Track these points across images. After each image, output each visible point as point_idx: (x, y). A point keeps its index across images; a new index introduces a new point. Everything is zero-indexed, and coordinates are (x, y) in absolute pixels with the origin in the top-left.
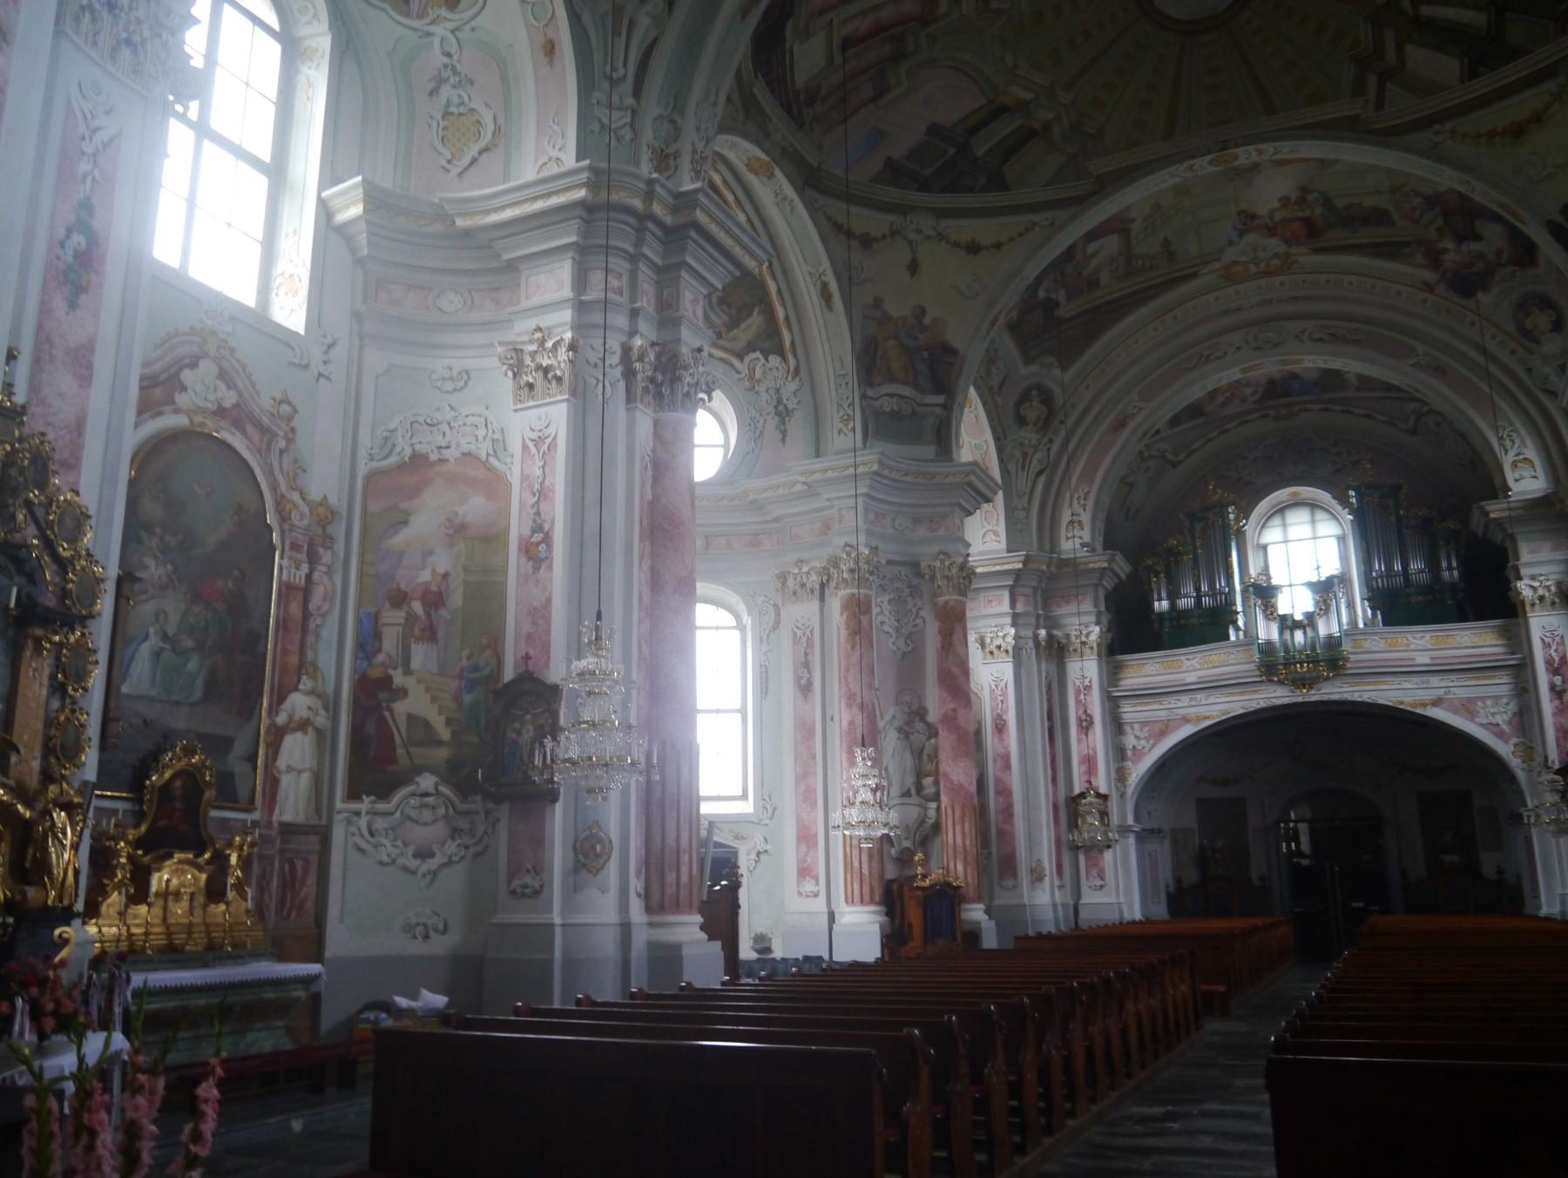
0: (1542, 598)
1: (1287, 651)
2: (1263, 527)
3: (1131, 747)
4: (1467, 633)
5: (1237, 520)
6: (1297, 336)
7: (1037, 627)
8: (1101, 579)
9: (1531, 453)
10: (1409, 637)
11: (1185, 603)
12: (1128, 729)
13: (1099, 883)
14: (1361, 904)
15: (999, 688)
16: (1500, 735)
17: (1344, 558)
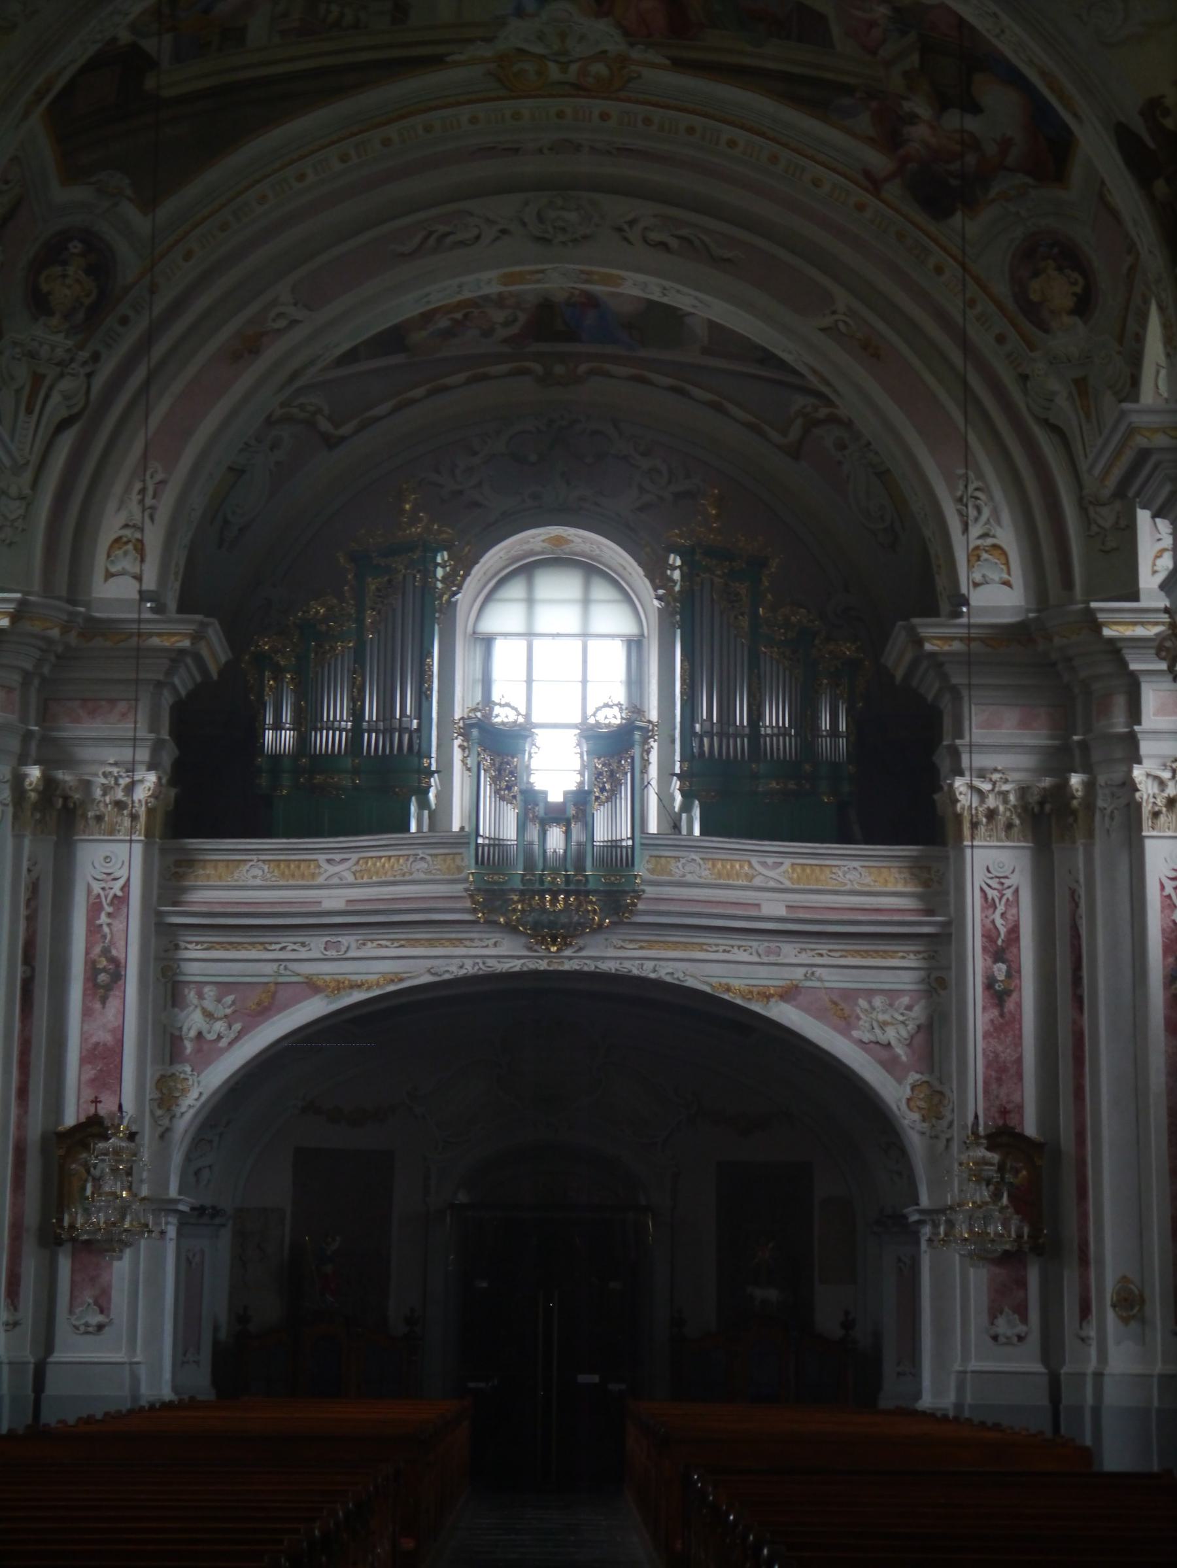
0: (991, 814)
1: (529, 865)
2: (488, 599)
3: (193, 1034)
4: (856, 864)
5: (449, 579)
6: (620, 230)
7: (23, 760)
8: (170, 672)
9: (1007, 536)
10: (754, 861)
11: (327, 741)
12: (191, 996)
13: (96, 1319)
14: (595, 1379)
16: (890, 1065)
17: (635, 682)
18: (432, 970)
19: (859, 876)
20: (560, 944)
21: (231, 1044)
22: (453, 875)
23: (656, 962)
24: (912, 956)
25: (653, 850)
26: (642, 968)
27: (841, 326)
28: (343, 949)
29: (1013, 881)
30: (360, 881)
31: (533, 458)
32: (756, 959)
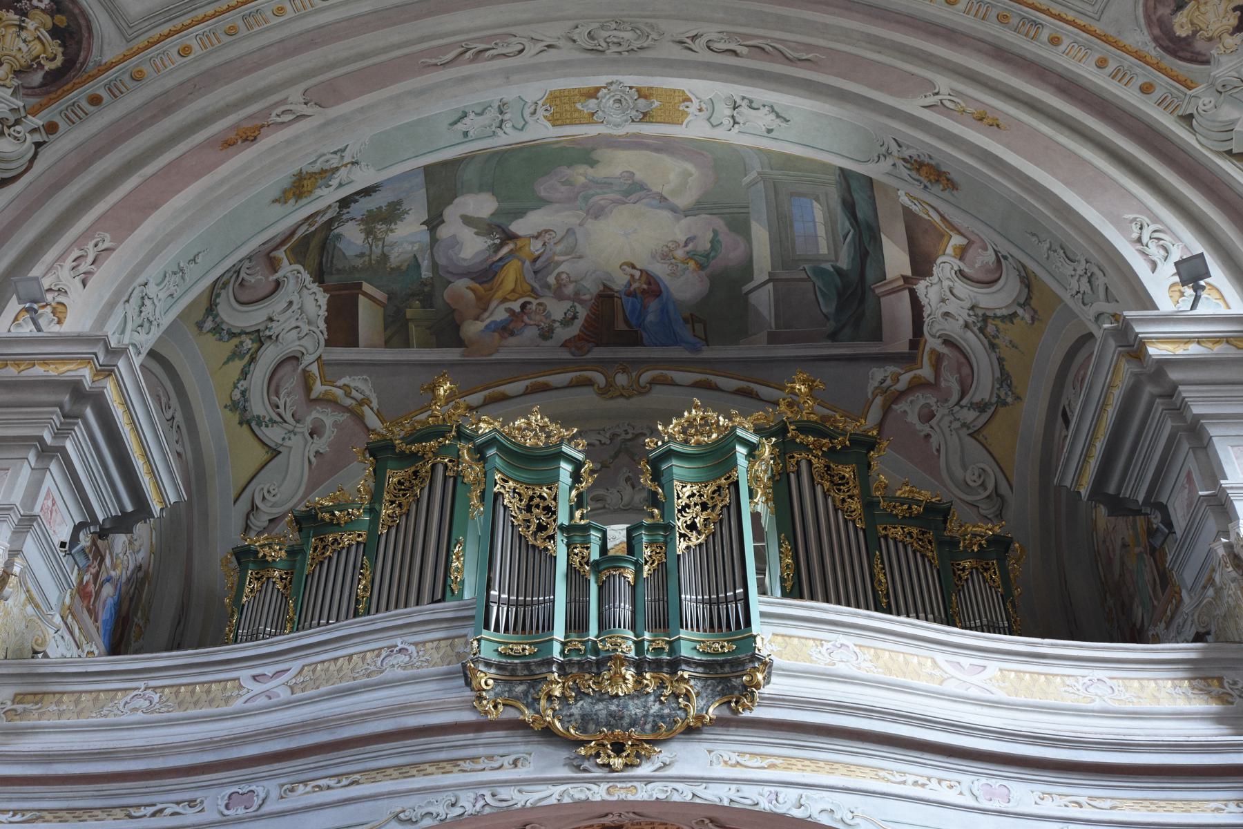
6: (681, 42)
18: (402, 815)
19: (1110, 691)
20: (628, 755)
22: (448, 664)
23: (800, 791)
24: (1232, 807)
25: (779, 625)
26: (776, 800)
27: (947, 103)
28: (257, 802)
30: (299, 695)
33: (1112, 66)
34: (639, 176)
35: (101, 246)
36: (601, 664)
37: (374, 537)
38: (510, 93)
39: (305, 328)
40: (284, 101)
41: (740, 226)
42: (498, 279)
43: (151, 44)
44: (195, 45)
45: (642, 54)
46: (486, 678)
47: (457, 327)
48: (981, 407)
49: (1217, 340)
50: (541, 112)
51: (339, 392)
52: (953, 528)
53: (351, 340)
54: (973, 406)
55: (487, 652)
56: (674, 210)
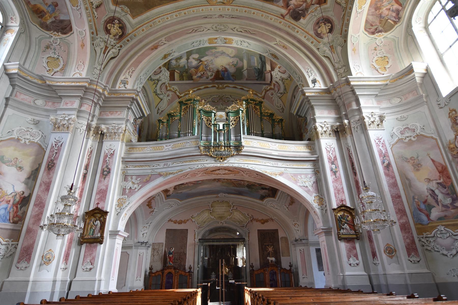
3: (129, 188)
6: (232, 29)
13: (89, 266)
14: (233, 281)
15: (57, 146)
16: (308, 192)
21: (138, 190)
28: (168, 165)
29: (333, 146)
31: (216, 101)
32: (272, 165)
33: (307, 38)
34: (224, 51)
35: (133, 70)
36: (219, 146)
37: (181, 118)
38: (201, 39)
39: (166, 78)
40: (161, 40)
41: (242, 60)
42: (199, 69)
43: (137, 29)
44: (145, 29)
45: (225, 32)
46: (202, 148)
47: (192, 77)
48: (281, 93)
49: (317, 93)
50: (207, 42)
51: (172, 89)
52: (274, 118)
53: (174, 80)
54: (280, 93)
55: (202, 144)
56: (230, 57)
